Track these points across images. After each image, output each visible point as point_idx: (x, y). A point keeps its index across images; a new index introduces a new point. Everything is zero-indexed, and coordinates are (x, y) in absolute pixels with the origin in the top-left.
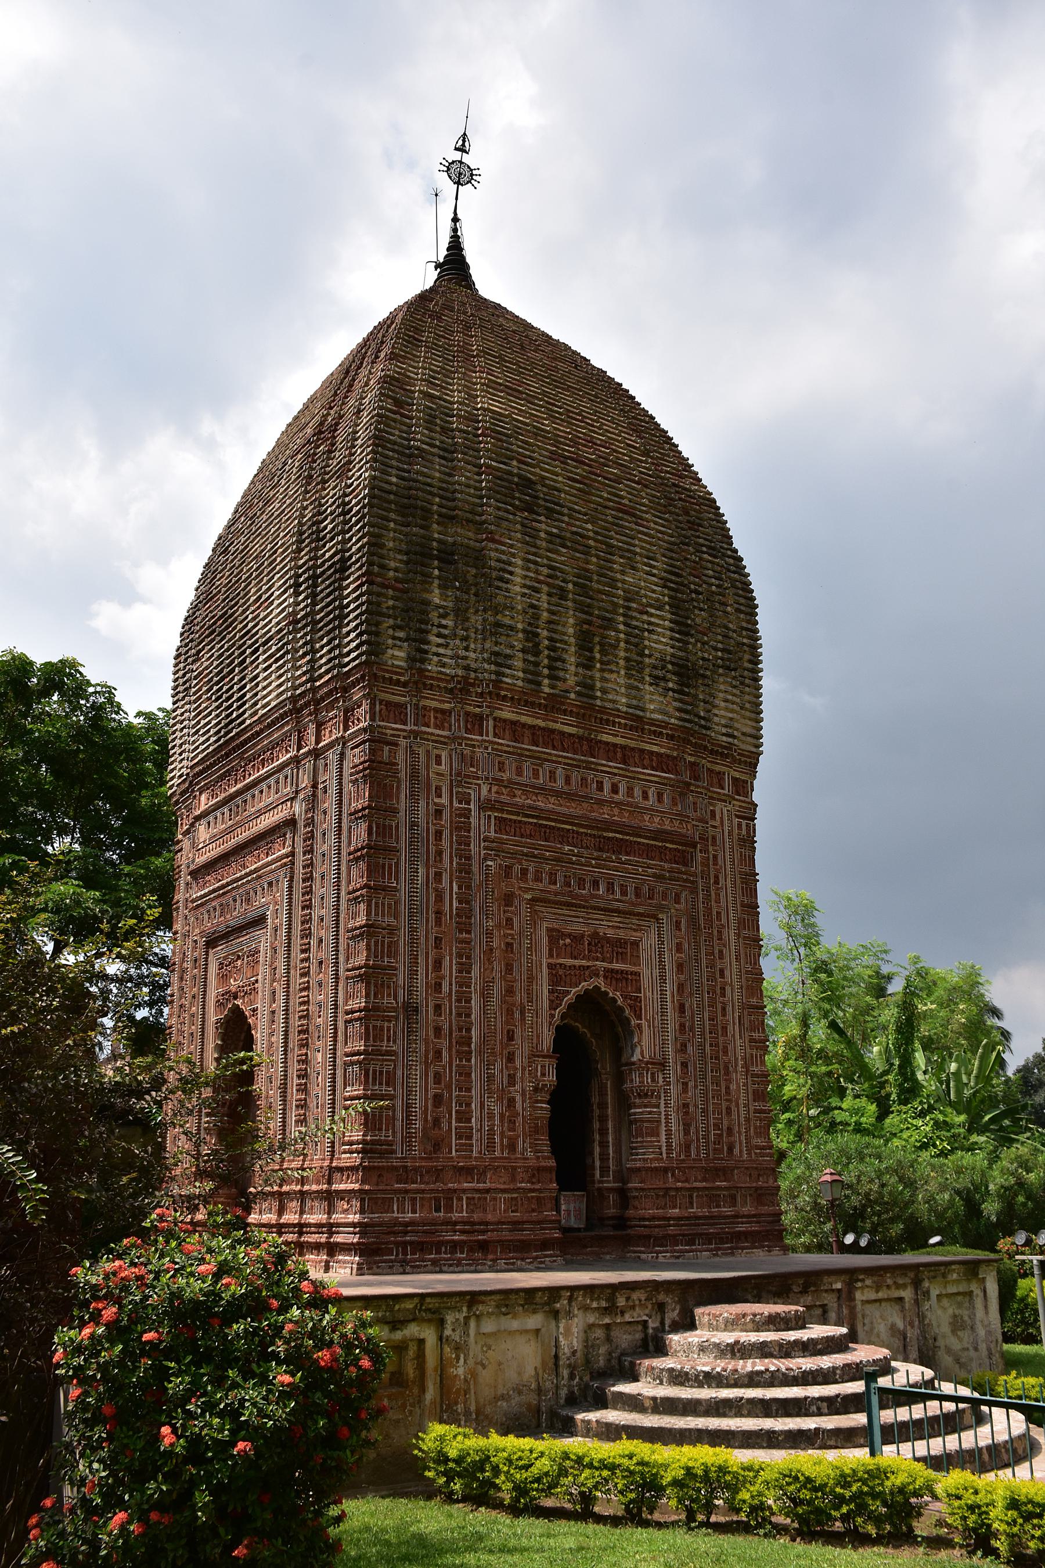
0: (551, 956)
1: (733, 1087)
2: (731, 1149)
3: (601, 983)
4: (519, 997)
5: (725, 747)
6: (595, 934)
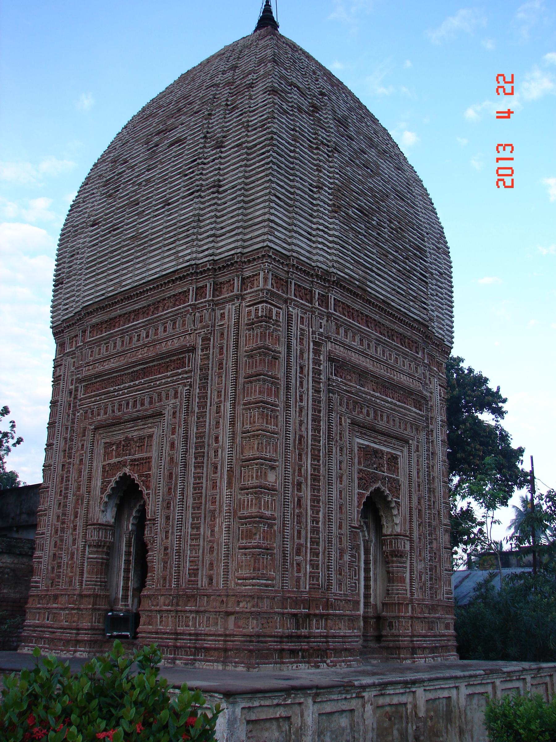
0: (104, 460)
1: (216, 529)
2: (211, 579)
3: (127, 470)
4: (83, 489)
5: (229, 260)
6: (127, 438)
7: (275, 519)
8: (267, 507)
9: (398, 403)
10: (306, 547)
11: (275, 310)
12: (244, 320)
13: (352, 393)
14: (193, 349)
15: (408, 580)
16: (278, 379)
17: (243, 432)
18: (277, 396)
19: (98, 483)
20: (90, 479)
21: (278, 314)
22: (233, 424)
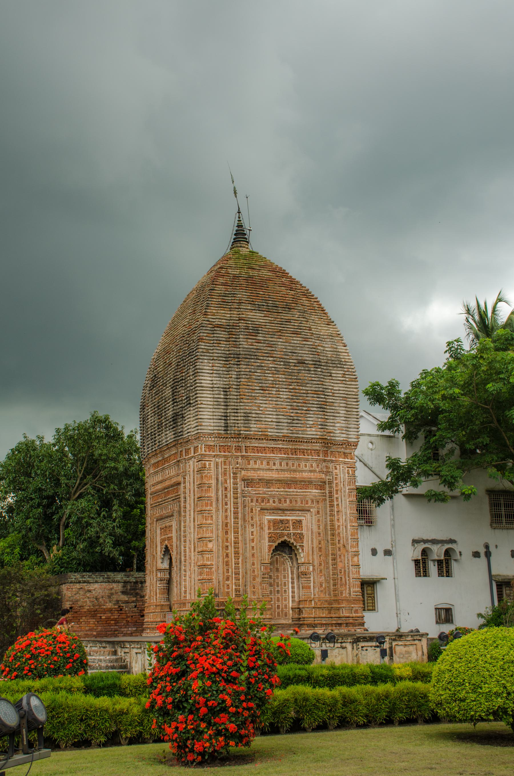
7: (213, 565)
8: (208, 559)
9: (299, 491)
10: (232, 577)
11: (207, 463)
12: (196, 470)
13: (260, 494)
14: (179, 484)
15: (312, 587)
16: (211, 497)
17: (198, 525)
18: (211, 505)
19: (159, 549)
20: (156, 547)
21: (210, 464)
22: (194, 521)
